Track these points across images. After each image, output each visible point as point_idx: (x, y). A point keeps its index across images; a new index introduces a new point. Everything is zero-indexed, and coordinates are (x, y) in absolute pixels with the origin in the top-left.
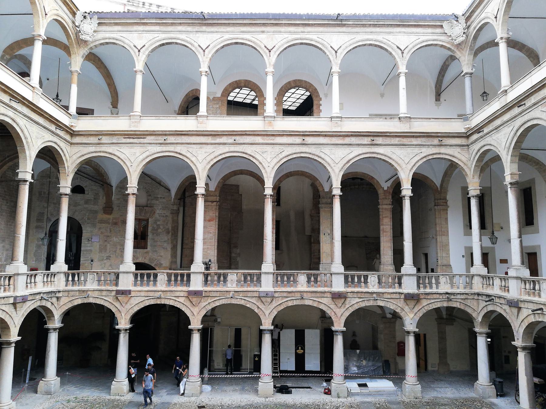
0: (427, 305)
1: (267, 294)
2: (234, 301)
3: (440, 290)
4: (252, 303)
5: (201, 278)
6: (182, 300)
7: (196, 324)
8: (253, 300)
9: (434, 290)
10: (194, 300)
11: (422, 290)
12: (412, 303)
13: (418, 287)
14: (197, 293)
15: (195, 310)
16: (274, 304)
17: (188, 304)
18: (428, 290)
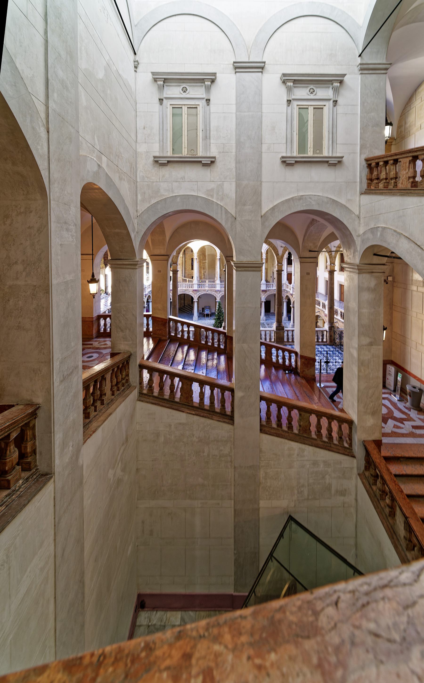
0: (268, 293)
1: (218, 291)
2: (208, 293)
3: (273, 289)
4: (213, 293)
5: (197, 285)
6: (191, 292)
7: (195, 300)
8: (214, 292)
9: (271, 289)
10: (195, 292)
11: (267, 289)
12: (264, 293)
13: (266, 287)
14: (195, 290)
15: (196, 295)
16: (220, 294)
17: (193, 293)
18: (269, 289)
